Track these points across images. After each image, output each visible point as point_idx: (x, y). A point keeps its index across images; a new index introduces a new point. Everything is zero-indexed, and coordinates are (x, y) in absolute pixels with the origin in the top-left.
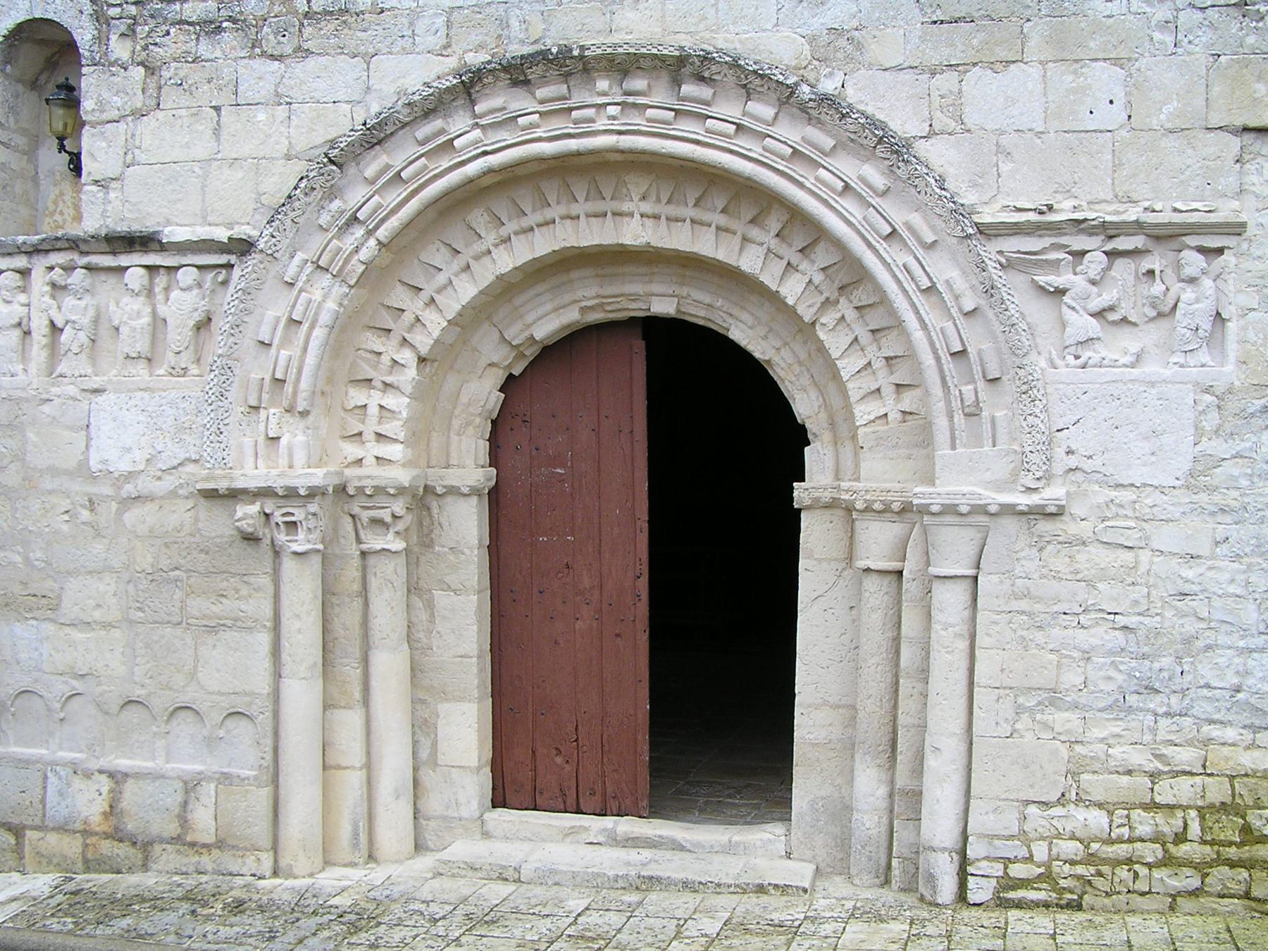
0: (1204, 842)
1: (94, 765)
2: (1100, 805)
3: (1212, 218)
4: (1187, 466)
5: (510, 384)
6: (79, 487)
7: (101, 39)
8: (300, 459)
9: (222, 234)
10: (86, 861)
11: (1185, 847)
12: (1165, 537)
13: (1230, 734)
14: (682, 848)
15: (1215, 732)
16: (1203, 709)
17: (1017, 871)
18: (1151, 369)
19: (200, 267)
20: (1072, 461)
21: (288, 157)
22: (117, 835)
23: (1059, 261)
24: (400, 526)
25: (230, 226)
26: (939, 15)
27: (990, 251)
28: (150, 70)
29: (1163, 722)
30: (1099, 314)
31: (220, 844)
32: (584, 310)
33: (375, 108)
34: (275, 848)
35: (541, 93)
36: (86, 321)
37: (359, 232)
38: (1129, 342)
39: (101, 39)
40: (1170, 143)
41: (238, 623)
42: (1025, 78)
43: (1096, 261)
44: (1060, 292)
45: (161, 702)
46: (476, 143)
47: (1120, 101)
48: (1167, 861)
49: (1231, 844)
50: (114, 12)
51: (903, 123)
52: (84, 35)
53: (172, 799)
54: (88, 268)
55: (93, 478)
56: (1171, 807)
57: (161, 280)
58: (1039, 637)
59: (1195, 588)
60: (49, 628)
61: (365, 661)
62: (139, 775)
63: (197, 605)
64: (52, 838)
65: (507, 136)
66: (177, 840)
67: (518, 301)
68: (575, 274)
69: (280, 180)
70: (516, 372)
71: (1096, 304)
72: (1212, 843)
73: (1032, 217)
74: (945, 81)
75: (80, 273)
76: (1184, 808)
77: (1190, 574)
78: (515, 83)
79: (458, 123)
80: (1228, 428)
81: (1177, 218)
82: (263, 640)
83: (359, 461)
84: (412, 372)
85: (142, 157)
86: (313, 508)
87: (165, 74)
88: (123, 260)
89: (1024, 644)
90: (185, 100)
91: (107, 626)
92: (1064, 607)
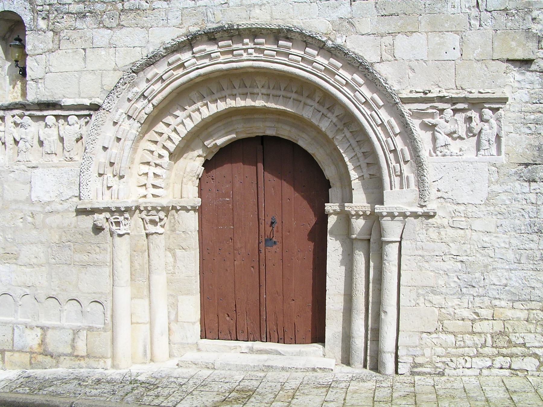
0: (493, 347)
1: (34, 324)
3: (495, 96)
4: (485, 196)
6: (27, 208)
9: (87, 102)
10: (31, 363)
11: (486, 349)
12: (477, 225)
13: (503, 303)
14: (280, 354)
15: (497, 302)
17: (419, 360)
20: (439, 194)
21: (115, 70)
25: (91, 98)
28: (56, 33)
29: (476, 299)
30: (450, 135)
31: (88, 356)
33: (151, 50)
34: (113, 357)
35: (221, 44)
39: (34, 19)
42: (419, 39)
43: (449, 112)
44: (434, 126)
46: (194, 64)
47: (458, 48)
48: (478, 355)
49: (504, 347)
50: (39, 8)
52: (27, 18)
54: (30, 116)
55: (32, 203)
56: (479, 333)
58: (426, 265)
59: (489, 245)
60: (15, 266)
62: (54, 328)
63: (78, 257)
64: (17, 355)
66: (71, 355)
67: (210, 130)
68: (234, 118)
69: (111, 80)
72: (496, 347)
73: (422, 95)
74: (388, 40)
75: (26, 118)
76: (485, 334)
77: (486, 239)
79: (186, 56)
80: (501, 180)
81: (481, 96)
82: (107, 270)
83: (145, 196)
84: (167, 158)
85: (52, 70)
87: (62, 35)
88: (45, 113)
89: (420, 268)
90: (70, 46)
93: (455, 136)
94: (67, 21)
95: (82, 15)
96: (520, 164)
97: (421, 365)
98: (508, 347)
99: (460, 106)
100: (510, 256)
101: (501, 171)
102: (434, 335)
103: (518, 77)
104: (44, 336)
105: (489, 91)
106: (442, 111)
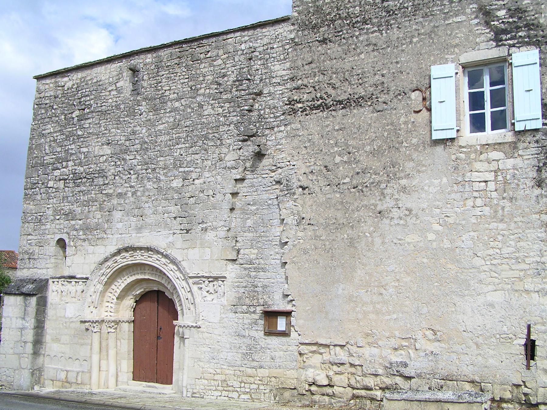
1: (64, 369)
2: (206, 379)
3: (221, 275)
4: (219, 319)
5: (136, 302)
7: (69, 242)
8: (96, 315)
9: (84, 276)
12: (216, 332)
13: (225, 367)
14: (156, 388)
15: (223, 366)
16: (221, 362)
17: (195, 391)
18: (215, 301)
19: (83, 282)
22: (67, 382)
24: (114, 328)
25: (86, 275)
26: (184, 240)
27: (191, 281)
28: (76, 247)
30: (208, 292)
31: (81, 384)
32: (145, 289)
35: (130, 253)
36: (66, 291)
37: (104, 276)
38: (212, 296)
39: (69, 242)
40: (216, 262)
41: (86, 344)
42: (196, 250)
43: (207, 282)
45: (74, 358)
47: (210, 254)
48: (216, 390)
50: (71, 237)
51: (179, 258)
52: (67, 241)
53: (75, 375)
54: (67, 281)
55: (66, 318)
56: (217, 380)
57: (77, 284)
58: (198, 349)
60: (59, 344)
61: (107, 352)
62: (71, 371)
64: (58, 382)
65: (125, 260)
67: (135, 287)
69: (93, 267)
70: (137, 299)
71: (207, 290)
72: (223, 387)
73: (196, 275)
76: (219, 380)
77: (219, 338)
78: (126, 251)
79: (118, 258)
81: (218, 275)
82: (89, 347)
84: (115, 300)
86: (97, 324)
88: (71, 280)
90: (80, 253)
91: (67, 344)
92: (201, 344)
94: (79, 243)
95: (84, 240)
96: (232, 305)
97: (195, 393)
98: (227, 387)
99: (210, 280)
100: (228, 346)
101: (225, 308)
102: (200, 380)
103: (231, 267)
104: (67, 374)
105: (219, 273)
106: (204, 282)
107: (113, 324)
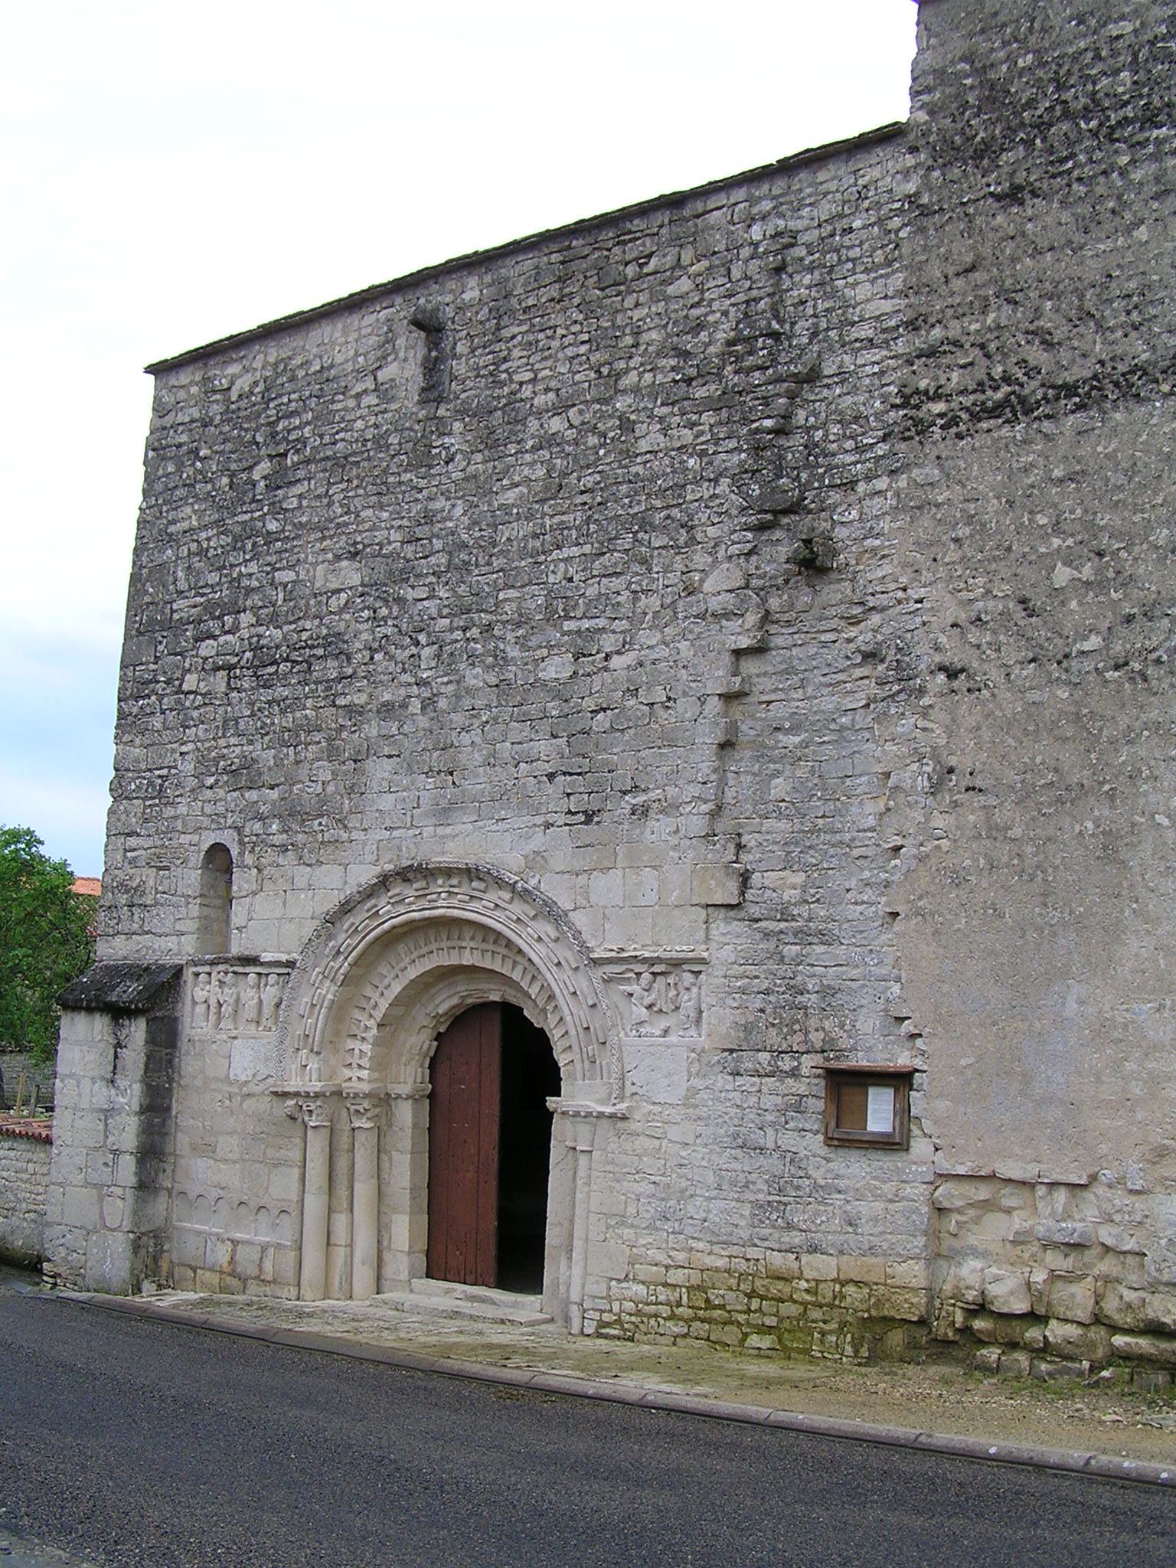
0: (689, 1307)
2: (643, 1283)
5: (439, 1037)
6: (225, 1088)
7: (241, 854)
9: (284, 958)
10: (220, 1287)
11: (680, 1309)
12: (674, 1133)
13: (701, 1245)
14: (495, 1304)
16: (689, 1230)
17: (606, 1317)
18: (672, 1038)
20: (634, 1089)
21: (312, 918)
22: (233, 1274)
23: (629, 978)
24: (369, 1115)
27: (600, 972)
29: (671, 1237)
30: (649, 1007)
31: (274, 1281)
33: (348, 892)
34: (299, 1285)
35: (415, 886)
36: (231, 1001)
39: (241, 854)
40: (676, 912)
43: (646, 977)
45: (254, 1204)
46: (389, 912)
48: (673, 1317)
49: (701, 1309)
51: (565, 903)
52: (234, 852)
54: (233, 972)
56: (675, 1286)
58: (617, 1186)
59: (686, 1162)
63: (271, 1153)
64: (208, 1274)
66: (257, 1278)
68: (457, 978)
69: (308, 929)
71: (647, 1001)
73: (614, 954)
74: (582, 879)
75: (230, 975)
76: (680, 1287)
77: (684, 1154)
78: (404, 881)
80: (703, 1072)
81: (682, 955)
82: (296, 1172)
83: (350, 1079)
84: (374, 1031)
85: (255, 916)
87: (266, 873)
88: (247, 970)
89: (611, 1189)
90: (272, 887)
91: (234, 1162)
93: (655, 1009)
94: (270, 856)
95: (283, 849)
96: (724, 1050)
97: (608, 1325)
98: (706, 1309)
99: (657, 969)
100: (711, 1179)
101: (704, 1060)
102: (624, 1285)
103: (723, 928)
104: (234, 1251)
105: (684, 948)
106: (639, 974)
107: (366, 1104)
